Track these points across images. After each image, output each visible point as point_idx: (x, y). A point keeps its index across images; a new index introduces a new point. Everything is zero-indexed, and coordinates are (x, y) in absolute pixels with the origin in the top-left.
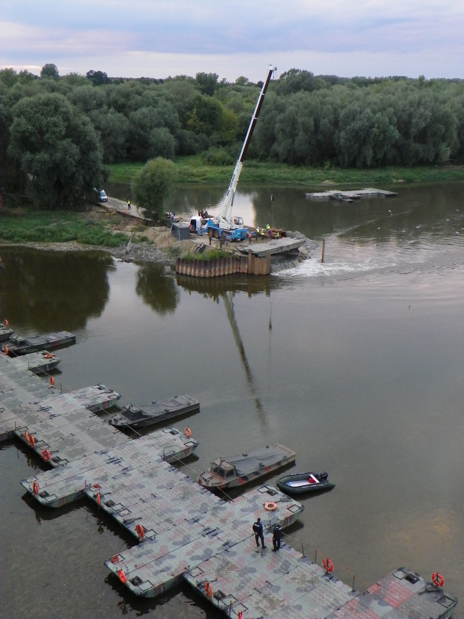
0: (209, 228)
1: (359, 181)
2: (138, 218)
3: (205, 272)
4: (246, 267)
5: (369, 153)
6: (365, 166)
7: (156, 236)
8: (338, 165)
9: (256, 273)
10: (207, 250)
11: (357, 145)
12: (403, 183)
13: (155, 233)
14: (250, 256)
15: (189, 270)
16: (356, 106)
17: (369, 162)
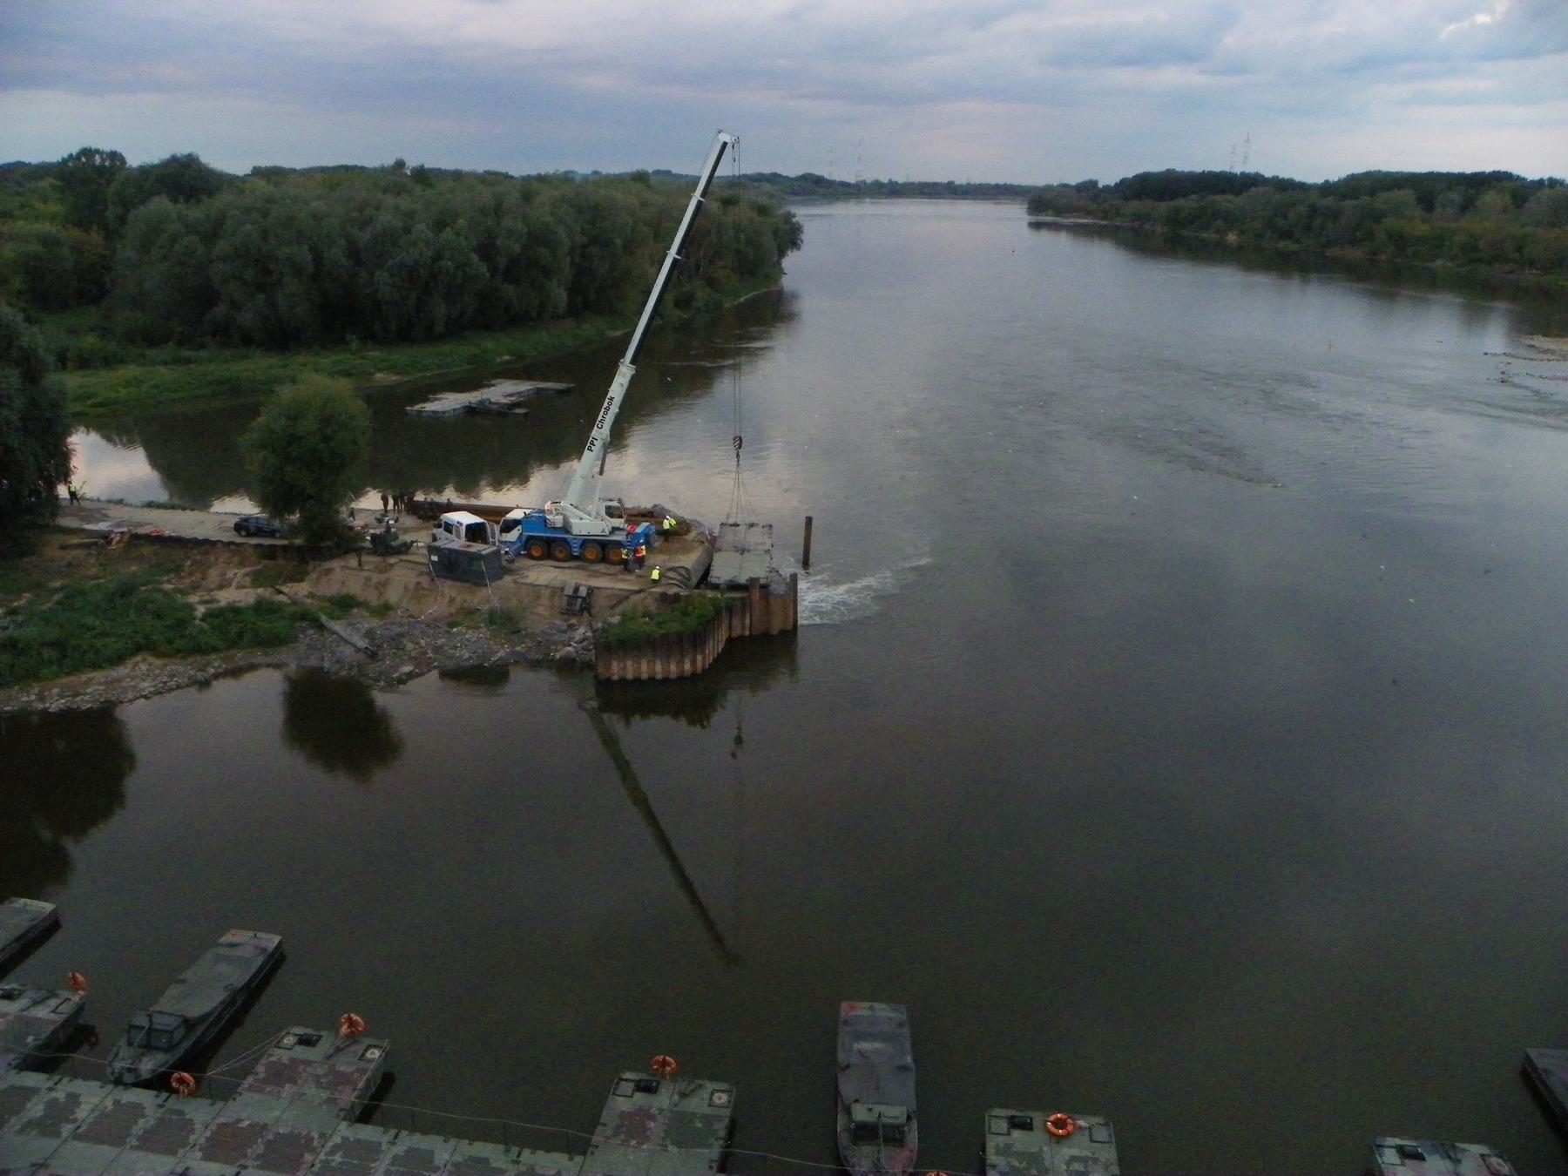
0: (530, 538)
1: (440, 366)
2: (230, 543)
3: (694, 663)
4: (748, 621)
5: (440, 310)
6: (431, 337)
7: (382, 586)
8: (371, 337)
9: (775, 632)
10: (600, 602)
11: (413, 296)
12: (507, 362)
13: (368, 579)
14: (756, 594)
15: (644, 667)
16: (386, 219)
17: (439, 328)
